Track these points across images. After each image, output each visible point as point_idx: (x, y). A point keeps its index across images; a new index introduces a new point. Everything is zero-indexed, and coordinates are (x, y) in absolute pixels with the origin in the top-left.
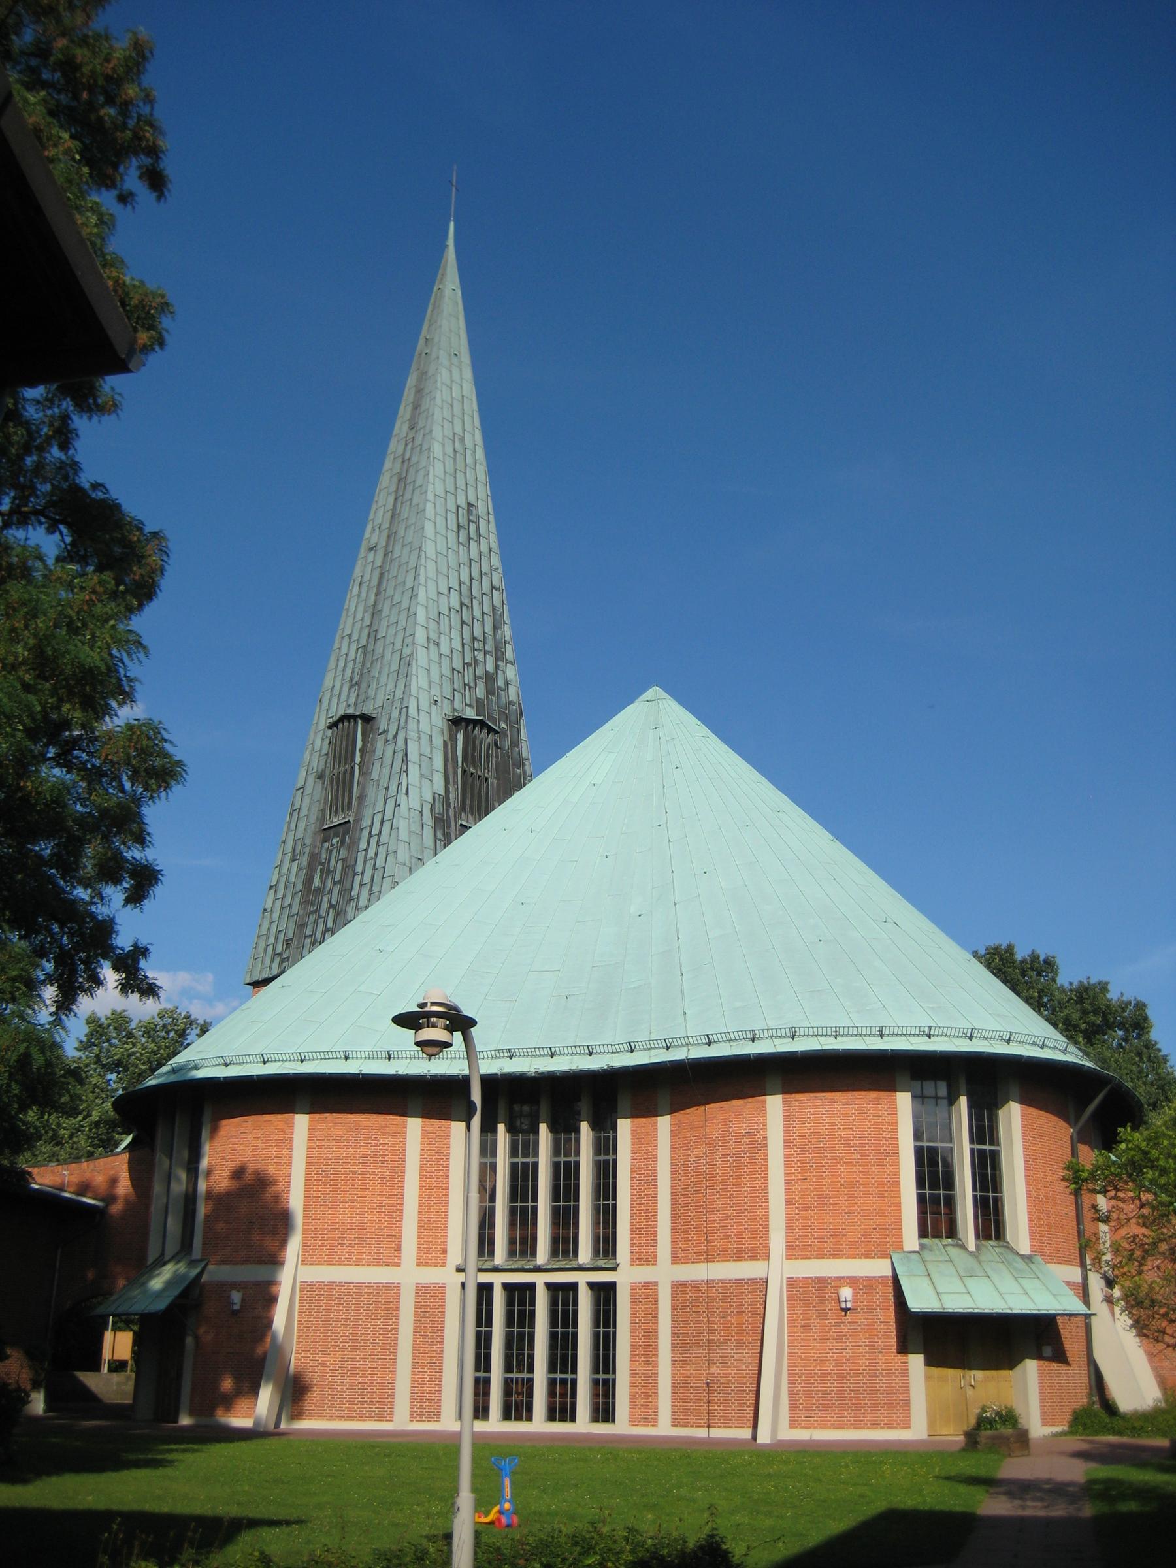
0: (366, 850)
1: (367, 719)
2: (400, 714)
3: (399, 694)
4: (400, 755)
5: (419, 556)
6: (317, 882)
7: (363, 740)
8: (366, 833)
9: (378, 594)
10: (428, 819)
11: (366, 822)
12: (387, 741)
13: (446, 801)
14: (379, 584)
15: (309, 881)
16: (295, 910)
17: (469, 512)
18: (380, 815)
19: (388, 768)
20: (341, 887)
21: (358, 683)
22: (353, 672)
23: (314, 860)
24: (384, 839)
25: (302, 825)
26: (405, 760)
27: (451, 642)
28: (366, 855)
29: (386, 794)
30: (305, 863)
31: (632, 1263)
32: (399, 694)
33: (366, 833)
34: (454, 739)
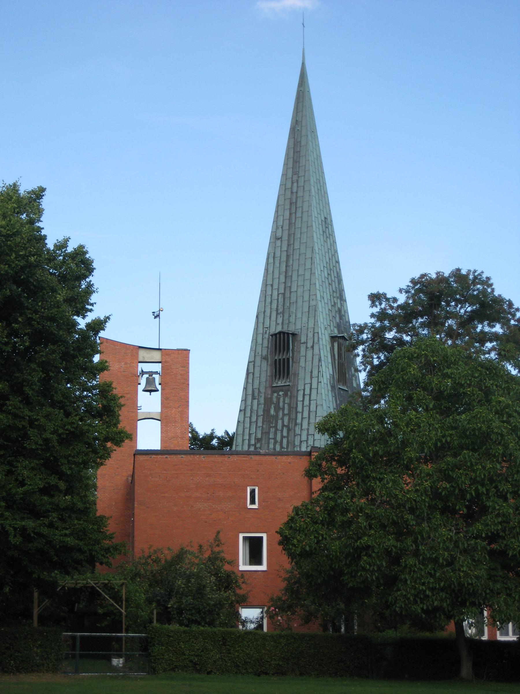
0: (303, 401)
1: (294, 335)
2: (314, 336)
3: (311, 324)
4: (317, 357)
5: (312, 252)
6: (272, 412)
7: (292, 345)
8: (301, 393)
9: (287, 266)
10: (330, 388)
11: (301, 387)
12: (307, 348)
13: (333, 375)
14: (287, 261)
15: (266, 411)
16: (260, 424)
17: (325, 222)
18: (309, 385)
19: (310, 362)
20: (289, 417)
21: (283, 313)
22: (277, 306)
23: (268, 402)
24: (313, 396)
25: (256, 382)
26: (320, 360)
27: (327, 296)
28: (303, 404)
29: (311, 375)
30: (262, 400)
31: (243, 565)
32: (311, 324)
33: (301, 393)
34: (333, 346)
